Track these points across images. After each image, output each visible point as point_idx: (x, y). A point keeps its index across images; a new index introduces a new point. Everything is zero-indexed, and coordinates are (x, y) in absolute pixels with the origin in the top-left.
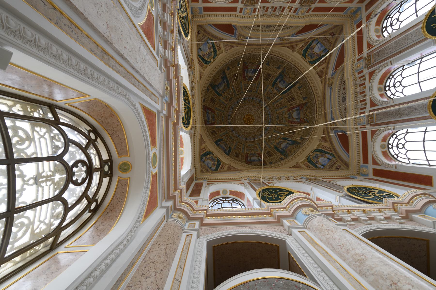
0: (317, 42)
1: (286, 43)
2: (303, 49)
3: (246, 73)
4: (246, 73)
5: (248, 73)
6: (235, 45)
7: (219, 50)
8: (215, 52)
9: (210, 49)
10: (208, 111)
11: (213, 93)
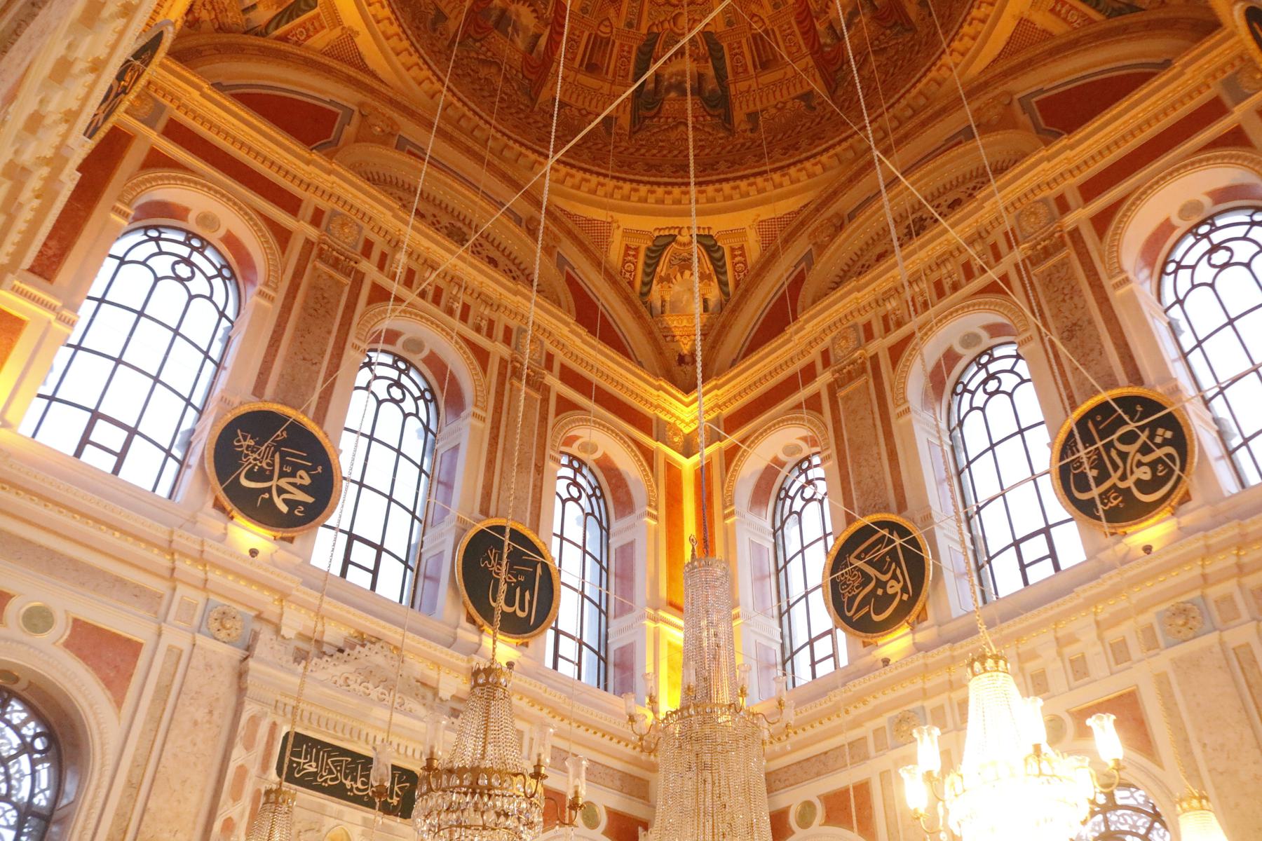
0: (252, 15)
1: (372, 91)
2: (312, 19)
3: (543, 41)
4: (543, 41)
5: (532, 30)
6: (570, 224)
7: (637, 249)
8: (655, 254)
9: (667, 279)
10: (826, 40)
11: (742, 86)
